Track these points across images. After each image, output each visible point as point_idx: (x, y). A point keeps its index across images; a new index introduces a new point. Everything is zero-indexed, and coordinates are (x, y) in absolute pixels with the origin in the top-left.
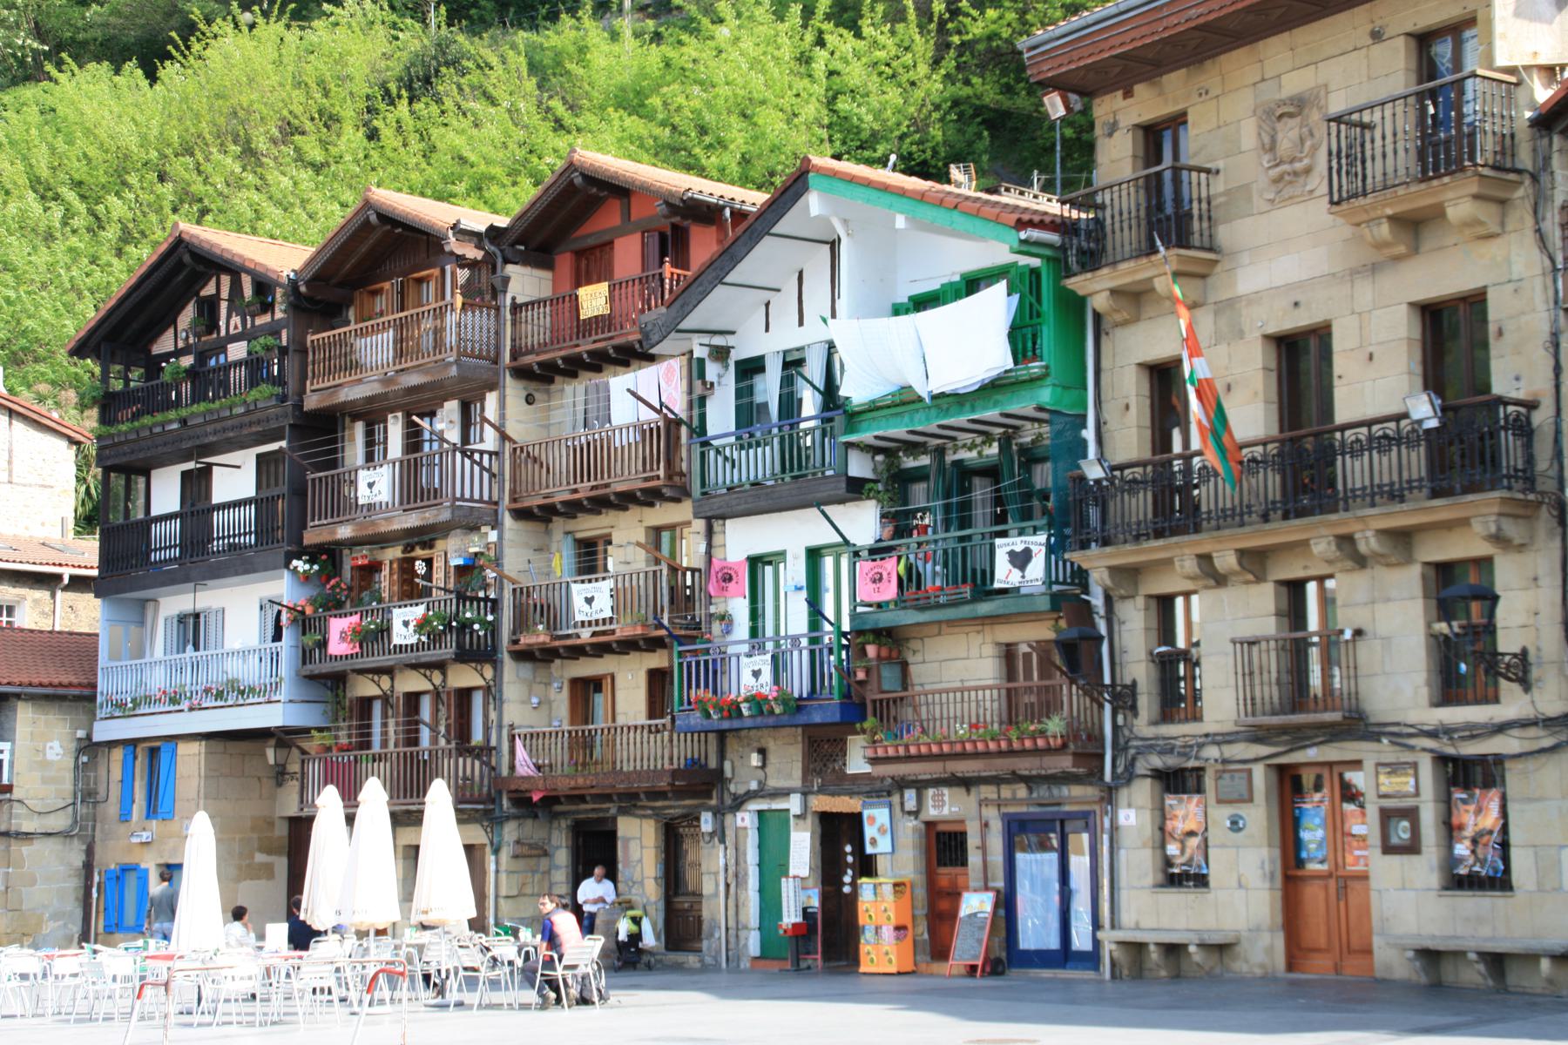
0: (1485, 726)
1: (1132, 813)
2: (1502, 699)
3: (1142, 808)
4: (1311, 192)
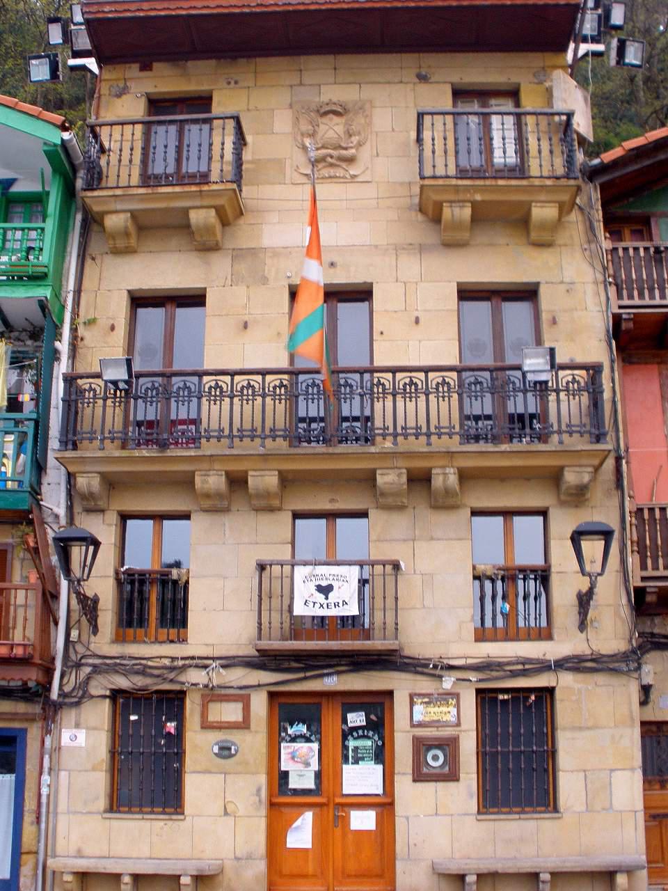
0: (538, 661)
1: (82, 735)
2: (555, 636)
3: (95, 729)
4: (354, 177)
